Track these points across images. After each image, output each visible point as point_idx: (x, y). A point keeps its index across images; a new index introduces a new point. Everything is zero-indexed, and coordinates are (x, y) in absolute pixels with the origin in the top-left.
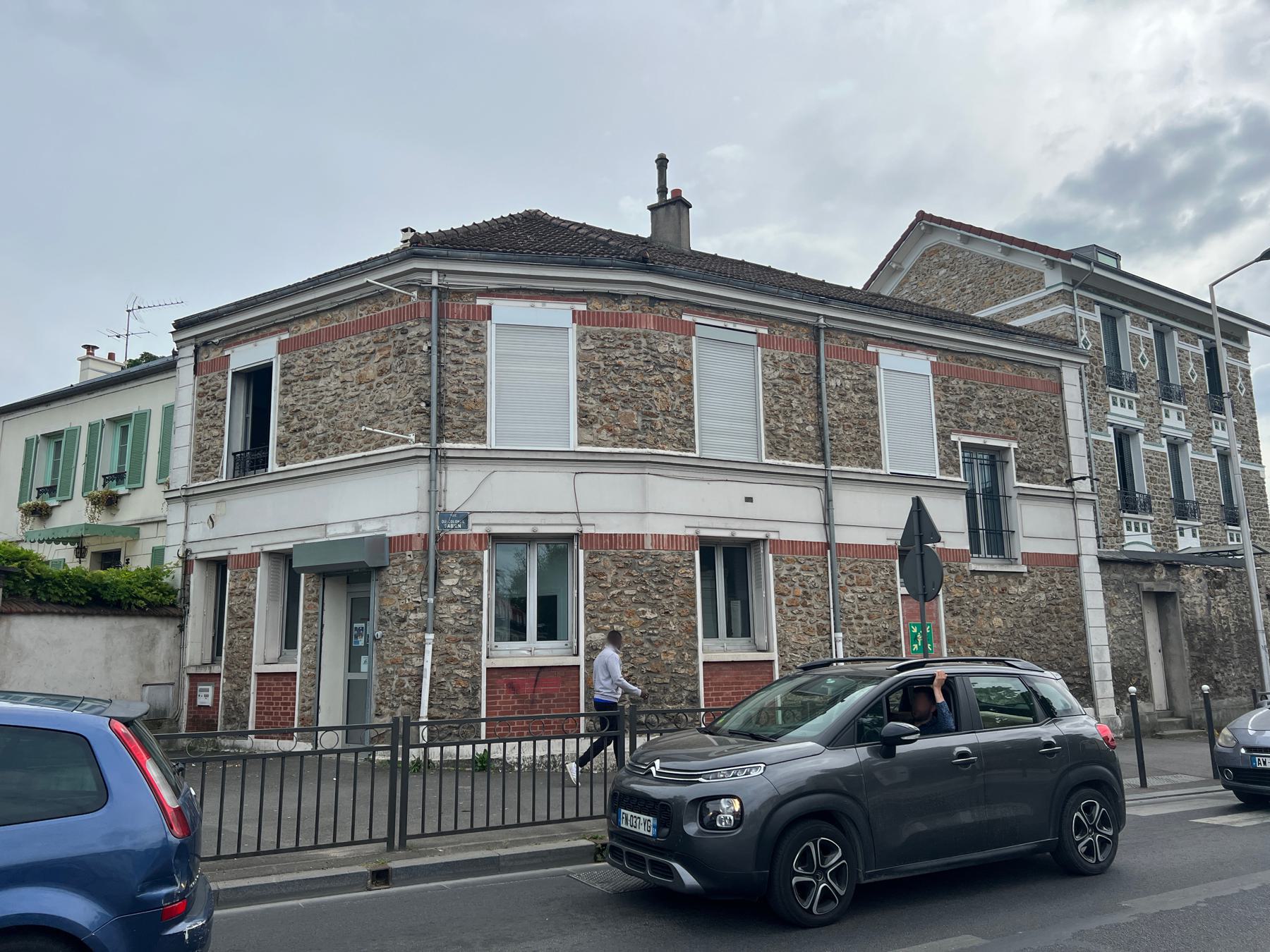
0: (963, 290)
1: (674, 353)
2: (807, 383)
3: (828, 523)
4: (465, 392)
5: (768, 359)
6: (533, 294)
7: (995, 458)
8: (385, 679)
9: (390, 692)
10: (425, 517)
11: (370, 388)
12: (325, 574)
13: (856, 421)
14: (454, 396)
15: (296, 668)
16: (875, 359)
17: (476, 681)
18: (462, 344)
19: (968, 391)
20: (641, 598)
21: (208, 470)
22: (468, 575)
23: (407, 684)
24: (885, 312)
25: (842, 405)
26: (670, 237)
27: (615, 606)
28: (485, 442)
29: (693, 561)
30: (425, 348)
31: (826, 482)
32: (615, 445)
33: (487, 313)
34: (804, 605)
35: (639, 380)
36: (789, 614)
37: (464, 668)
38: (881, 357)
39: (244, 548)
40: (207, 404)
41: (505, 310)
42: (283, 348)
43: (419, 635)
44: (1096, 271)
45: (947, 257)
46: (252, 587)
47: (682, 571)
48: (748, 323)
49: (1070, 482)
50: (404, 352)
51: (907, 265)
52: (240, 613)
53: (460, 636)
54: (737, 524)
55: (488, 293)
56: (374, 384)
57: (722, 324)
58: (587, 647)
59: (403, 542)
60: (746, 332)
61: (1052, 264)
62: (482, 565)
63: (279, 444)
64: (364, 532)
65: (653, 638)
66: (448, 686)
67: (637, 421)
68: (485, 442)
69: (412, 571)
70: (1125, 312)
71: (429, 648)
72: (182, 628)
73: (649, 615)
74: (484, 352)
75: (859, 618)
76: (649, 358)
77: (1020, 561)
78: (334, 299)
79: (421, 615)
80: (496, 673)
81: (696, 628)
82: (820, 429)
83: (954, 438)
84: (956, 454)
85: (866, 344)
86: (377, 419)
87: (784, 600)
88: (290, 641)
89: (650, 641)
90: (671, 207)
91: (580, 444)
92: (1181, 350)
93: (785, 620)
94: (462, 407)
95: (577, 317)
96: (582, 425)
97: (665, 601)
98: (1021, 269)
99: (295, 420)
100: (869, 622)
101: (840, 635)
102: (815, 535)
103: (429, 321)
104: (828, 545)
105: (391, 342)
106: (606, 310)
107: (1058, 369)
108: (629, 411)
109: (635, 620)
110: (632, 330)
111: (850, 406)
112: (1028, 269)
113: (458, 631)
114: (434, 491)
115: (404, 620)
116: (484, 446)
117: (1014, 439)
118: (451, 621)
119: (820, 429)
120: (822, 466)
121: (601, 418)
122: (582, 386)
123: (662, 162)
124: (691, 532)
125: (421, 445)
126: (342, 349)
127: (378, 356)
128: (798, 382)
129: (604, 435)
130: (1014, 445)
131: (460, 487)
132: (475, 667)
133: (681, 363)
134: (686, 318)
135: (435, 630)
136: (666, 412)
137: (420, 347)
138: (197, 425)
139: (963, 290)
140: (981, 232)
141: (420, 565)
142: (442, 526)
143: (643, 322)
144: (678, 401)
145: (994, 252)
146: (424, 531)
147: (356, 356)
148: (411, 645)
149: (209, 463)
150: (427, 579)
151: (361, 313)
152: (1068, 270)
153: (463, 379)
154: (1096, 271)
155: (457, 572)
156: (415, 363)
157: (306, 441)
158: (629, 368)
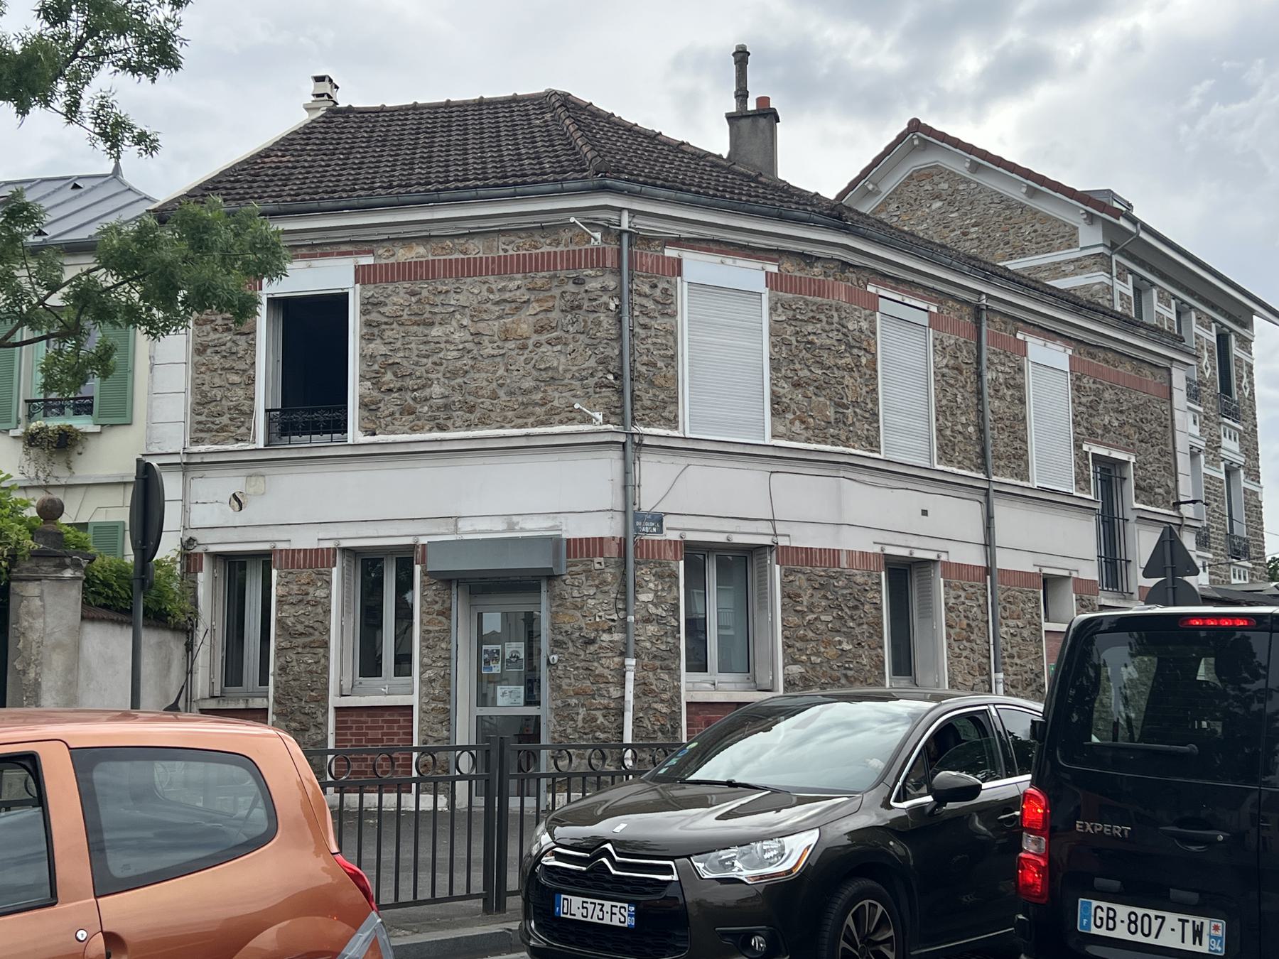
1: (861, 331)
4: (655, 365)
5: (937, 342)
6: (724, 248)
8: (564, 713)
9: (575, 729)
10: (619, 518)
11: (524, 347)
12: (447, 580)
14: (643, 369)
15: (414, 700)
17: (675, 717)
18: (650, 305)
20: (838, 625)
21: (223, 429)
22: (663, 590)
23: (601, 719)
27: (810, 634)
28: (676, 428)
30: (612, 306)
32: (808, 440)
33: (677, 267)
35: (830, 362)
37: (662, 701)
39: (305, 540)
40: (213, 336)
41: (698, 266)
42: (362, 275)
43: (616, 660)
46: (321, 593)
47: (870, 595)
48: (922, 298)
50: (579, 307)
52: (300, 628)
53: (658, 663)
55: (678, 242)
56: (531, 342)
57: (899, 298)
58: (785, 681)
59: (592, 546)
60: (917, 310)
62: (677, 578)
63: (363, 405)
64: (522, 530)
65: (850, 673)
66: (646, 723)
67: (830, 413)
68: (676, 428)
69: (604, 582)
71: (630, 676)
72: (189, 647)
73: (846, 647)
74: (674, 315)
76: (841, 336)
78: (460, 224)
79: (617, 637)
80: (693, 709)
86: (537, 388)
88: (370, 665)
89: (846, 676)
91: (774, 436)
94: (651, 383)
95: (774, 282)
96: (775, 413)
99: (389, 376)
103: (618, 271)
105: (556, 292)
106: (798, 274)
108: (822, 399)
109: (831, 652)
110: (825, 301)
113: (655, 657)
114: (629, 486)
115: (592, 642)
116: (675, 433)
118: (648, 645)
121: (793, 406)
122: (775, 366)
124: (877, 549)
125: (610, 427)
126: (472, 291)
127: (535, 308)
129: (798, 427)
131: (659, 481)
132: (674, 701)
133: (863, 345)
134: (871, 289)
135: (637, 656)
136: (855, 403)
137: (606, 305)
138: (196, 366)
141: (613, 575)
142: (637, 530)
144: (865, 389)
146: (618, 533)
147: (497, 303)
148: (606, 672)
149: (225, 420)
150: (625, 593)
151: (505, 248)
153: (652, 348)
155: (651, 585)
156: (599, 324)
158: (821, 347)
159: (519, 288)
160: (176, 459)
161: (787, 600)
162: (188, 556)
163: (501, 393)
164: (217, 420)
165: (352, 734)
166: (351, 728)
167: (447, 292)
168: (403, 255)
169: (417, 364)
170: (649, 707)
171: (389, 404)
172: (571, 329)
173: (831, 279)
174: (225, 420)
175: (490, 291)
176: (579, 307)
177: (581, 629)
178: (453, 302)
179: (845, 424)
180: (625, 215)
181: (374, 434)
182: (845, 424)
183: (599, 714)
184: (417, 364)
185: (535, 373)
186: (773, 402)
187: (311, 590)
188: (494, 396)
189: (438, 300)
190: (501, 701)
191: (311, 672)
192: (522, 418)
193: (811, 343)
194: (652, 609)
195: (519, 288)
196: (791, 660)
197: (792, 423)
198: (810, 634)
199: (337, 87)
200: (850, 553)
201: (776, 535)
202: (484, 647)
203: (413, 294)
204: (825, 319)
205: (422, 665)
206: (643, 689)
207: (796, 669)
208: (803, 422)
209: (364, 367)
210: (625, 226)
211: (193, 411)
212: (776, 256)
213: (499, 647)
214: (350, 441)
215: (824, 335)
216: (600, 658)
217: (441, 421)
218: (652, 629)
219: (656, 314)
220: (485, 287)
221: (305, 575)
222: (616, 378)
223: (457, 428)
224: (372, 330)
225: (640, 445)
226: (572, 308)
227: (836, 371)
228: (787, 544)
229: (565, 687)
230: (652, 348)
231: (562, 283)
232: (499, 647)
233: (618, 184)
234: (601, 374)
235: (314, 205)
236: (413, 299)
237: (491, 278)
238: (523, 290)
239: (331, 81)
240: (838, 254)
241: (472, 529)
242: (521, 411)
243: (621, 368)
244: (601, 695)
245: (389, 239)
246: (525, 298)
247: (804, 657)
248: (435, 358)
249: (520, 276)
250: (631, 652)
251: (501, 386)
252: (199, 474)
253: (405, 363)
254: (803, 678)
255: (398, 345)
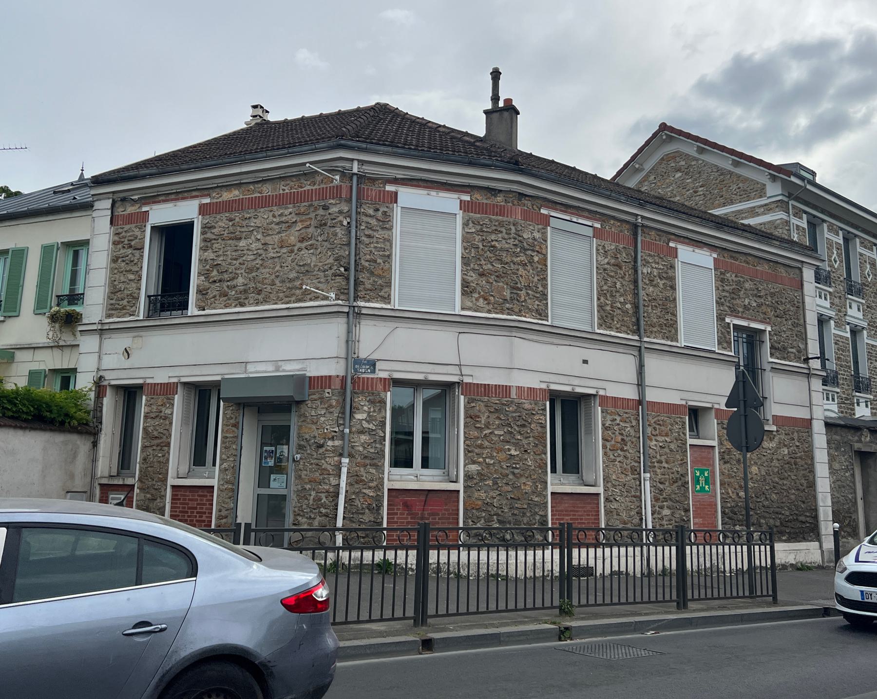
0: (696, 192)
1: (534, 239)
2: (627, 269)
3: (641, 384)
4: (375, 261)
5: (600, 248)
6: (429, 184)
7: (752, 338)
8: (302, 494)
9: (308, 505)
10: (342, 363)
11: (292, 251)
12: (242, 404)
13: (660, 302)
14: (367, 264)
15: (214, 482)
16: (674, 253)
17: (379, 499)
18: (373, 222)
19: (738, 283)
20: (508, 437)
21: (123, 308)
22: (374, 411)
23: (324, 500)
24: (684, 216)
25: (651, 289)
26: (502, 138)
27: (486, 443)
28: (389, 303)
29: (545, 410)
30: (345, 223)
31: (640, 351)
32: (489, 312)
33: (394, 197)
34: (622, 450)
35: (508, 260)
36: (612, 456)
37: (370, 488)
38: (679, 251)
39: (161, 377)
40: (122, 251)
41: (408, 196)
42: (203, 210)
43: (336, 459)
44: (809, 187)
45: (683, 163)
46: (168, 411)
47: (536, 417)
48: (587, 218)
49: (806, 360)
50: (325, 224)
51: (648, 166)
52: (156, 433)
53: (368, 462)
54: (576, 382)
55: (395, 181)
56: (296, 248)
57: (568, 218)
58: (465, 475)
59: (324, 381)
60: (585, 226)
61: (774, 178)
62: (385, 403)
63: (199, 291)
64: (284, 371)
65: (516, 471)
66: (357, 503)
67: (507, 294)
68: (389, 303)
69: (331, 406)
70: (824, 221)
71: (344, 470)
72: (95, 444)
73: (513, 452)
74: (390, 229)
75: (660, 462)
76: (517, 242)
77: (771, 422)
78: (258, 175)
79: (337, 443)
80: (394, 494)
81: (546, 464)
82: (636, 307)
83: (728, 320)
84: (729, 333)
85: (669, 240)
86: (298, 278)
87: (608, 445)
88: (199, 458)
90: (503, 114)
91: (463, 309)
92: (861, 255)
93: (609, 462)
94: (372, 273)
95: (464, 206)
96: (464, 293)
97: (525, 442)
98: (746, 180)
99: (215, 273)
100: (666, 466)
101: (648, 475)
102: (631, 393)
103: (350, 200)
104: (640, 402)
105: (312, 215)
106: (485, 201)
107: (800, 270)
108: (501, 284)
109: (502, 456)
110: (505, 219)
111: (657, 290)
112: (752, 180)
113: (366, 457)
114: (350, 341)
115: (321, 446)
116: (389, 307)
117: (768, 323)
118: (361, 449)
119: (636, 307)
120: (637, 338)
121: (479, 289)
122: (466, 261)
123: (496, 75)
124: (544, 386)
125: (340, 302)
126: (264, 217)
127: (299, 226)
128: (621, 268)
129: (481, 302)
130: (769, 329)
131: (371, 339)
132: (379, 487)
133: (538, 248)
134: (543, 211)
135: (350, 456)
136: (528, 287)
137: (341, 222)
138: (112, 269)
139: (696, 192)
140: (715, 145)
141: (337, 401)
142: (356, 370)
143: (513, 212)
144: (536, 279)
145: (726, 164)
146: (342, 373)
147: (278, 224)
148: (329, 467)
149: (125, 302)
150: (344, 413)
151: (284, 188)
152: (786, 184)
153: (373, 250)
154: (809, 187)
155: (365, 408)
156: (336, 235)
157: (221, 289)
158: (501, 250)
159: (291, 213)
160: (94, 327)
161: (469, 420)
162: (99, 386)
163: (277, 282)
164: (121, 303)
165: (181, 504)
166: (179, 499)
167: (250, 218)
168: (227, 196)
169: (230, 264)
170: (360, 492)
171: (214, 290)
172: (319, 238)
173: (510, 204)
174: (125, 302)
175: (274, 216)
176: (325, 224)
177: (315, 437)
178: (252, 224)
179: (518, 300)
180: (356, 164)
181: (204, 310)
182: (518, 300)
183: (323, 496)
184: (230, 264)
185: (297, 268)
186: (463, 286)
187: (163, 409)
188: (273, 284)
189: (244, 223)
190: (272, 484)
191: (159, 462)
192: (288, 296)
193: (494, 246)
194: (365, 425)
195: (291, 213)
196: (470, 461)
197: (477, 300)
198: (486, 443)
199: (267, 112)
200: (519, 388)
201: (462, 375)
202: (265, 448)
203: (231, 220)
204: (504, 231)
205: (221, 459)
206: (355, 479)
207: (474, 468)
208: (485, 299)
209: (201, 267)
210: (355, 170)
211: (109, 297)
212: (469, 190)
213: (273, 448)
214: (189, 314)
215: (504, 241)
216: (325, 458)
217: (242, 300)
218: (364, 438)
219: (378, 228)
220: (271, 214)
221: (160, 400)
222: (345, 270)
223: (250, 305)
224: (207, 244)
225: (360, 314)
226: (321, 225)
227: (512, 265)
228: (470, 381)
229: (303, 477)
230: (373, 250)
231: (316, 209)
232: (273, 448)
233: (350, 143)
234: (335, 268)
235: (177, 168)
236: (231, 224)
237: (275, 208)
238: (293, 215)
239: (262, 107)
240: (515, 187)
241: (257, 370)
242: (287, 293)
243: (349, 264)
244: (324, 483)
245: (217, 187)
246: (294, 220)
247: (481, 460)
248: (240, 261)
249: (291, 206)
250: (346, 454)
251: (277, 277)
252: (108, 336)
253: (224, 264)
254: (479, 474)
255: (221, 253)
